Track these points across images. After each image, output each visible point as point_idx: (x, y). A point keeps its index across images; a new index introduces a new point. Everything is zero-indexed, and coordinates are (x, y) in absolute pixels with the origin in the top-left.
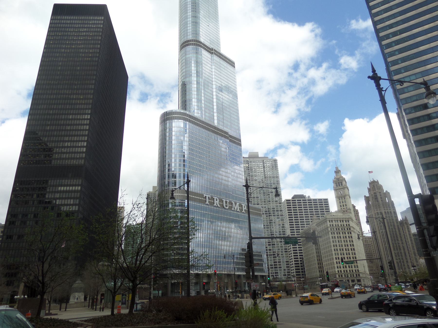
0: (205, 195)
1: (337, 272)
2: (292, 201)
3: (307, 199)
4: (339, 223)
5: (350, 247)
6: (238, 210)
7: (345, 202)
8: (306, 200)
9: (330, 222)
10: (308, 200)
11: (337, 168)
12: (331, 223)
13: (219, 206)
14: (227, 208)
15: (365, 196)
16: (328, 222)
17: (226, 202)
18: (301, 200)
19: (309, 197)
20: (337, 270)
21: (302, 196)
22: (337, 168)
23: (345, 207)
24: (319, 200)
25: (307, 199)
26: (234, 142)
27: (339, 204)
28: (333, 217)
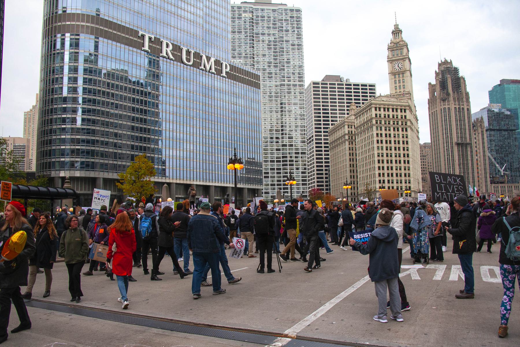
0: (141, 33)
2: (322, 84)
3: (344, 83)
4: (391, 113)
5: (402, 152)
6: (213, 70)
7: (403, 82)
8: (343, 85)
9: (376, 110)
10: (346, 85)
11: (396, 26)
13: (171, 57)
14: (191, 63)
15: (430, 84)
16: (373, 109)
17: (188, 53)
18: (335, 84)
21: (338, 78)
22: (396, 26)
23: (402, 90)
25: (344, 83)
27: (394, 85)
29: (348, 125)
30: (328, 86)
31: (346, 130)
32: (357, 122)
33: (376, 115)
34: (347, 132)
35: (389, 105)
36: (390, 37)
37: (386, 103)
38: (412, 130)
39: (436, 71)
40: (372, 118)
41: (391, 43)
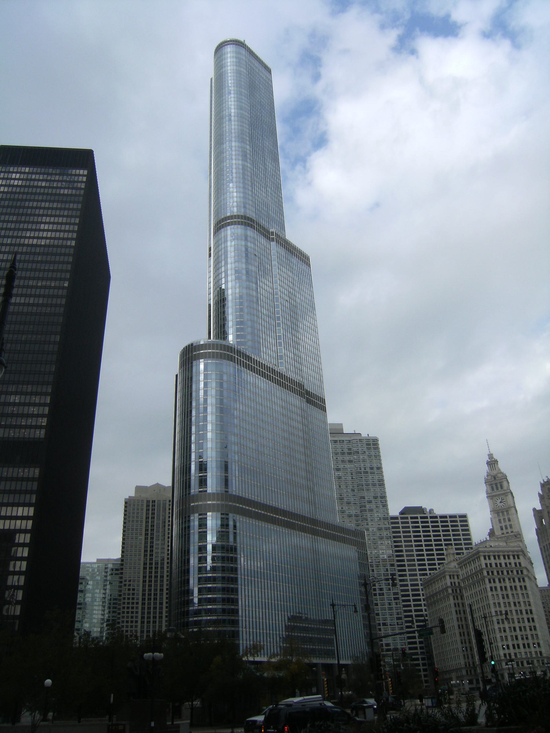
1: (503, 658)
2: (402, 518)
3: (429, 515)
4: (503, 561)
8: (427, 518)
9: (485, 559)
10: (431, 517)
11: (491, 456)
12: (488, 562)
15: (534, 510)
16: (482, 558)
18: (417, 518)
19: (431, 511)
20: (502, 653)
21: (420, 510)
22: (491, 456)
23: (509, 530)
24: (451, 517)
26: (315, 404)
28: (491, 549)
29: (450, 576)
30: (410, 520)
31: (448, 581)
32: (462, 573)
33: (486, 564)
34: (449, 584)
35: (498, 552)
36: (486, 468)
37: (496, 549)
38: (529, 578)
39: (539, 493)
40: (482, 569)
41: (487, 476)
